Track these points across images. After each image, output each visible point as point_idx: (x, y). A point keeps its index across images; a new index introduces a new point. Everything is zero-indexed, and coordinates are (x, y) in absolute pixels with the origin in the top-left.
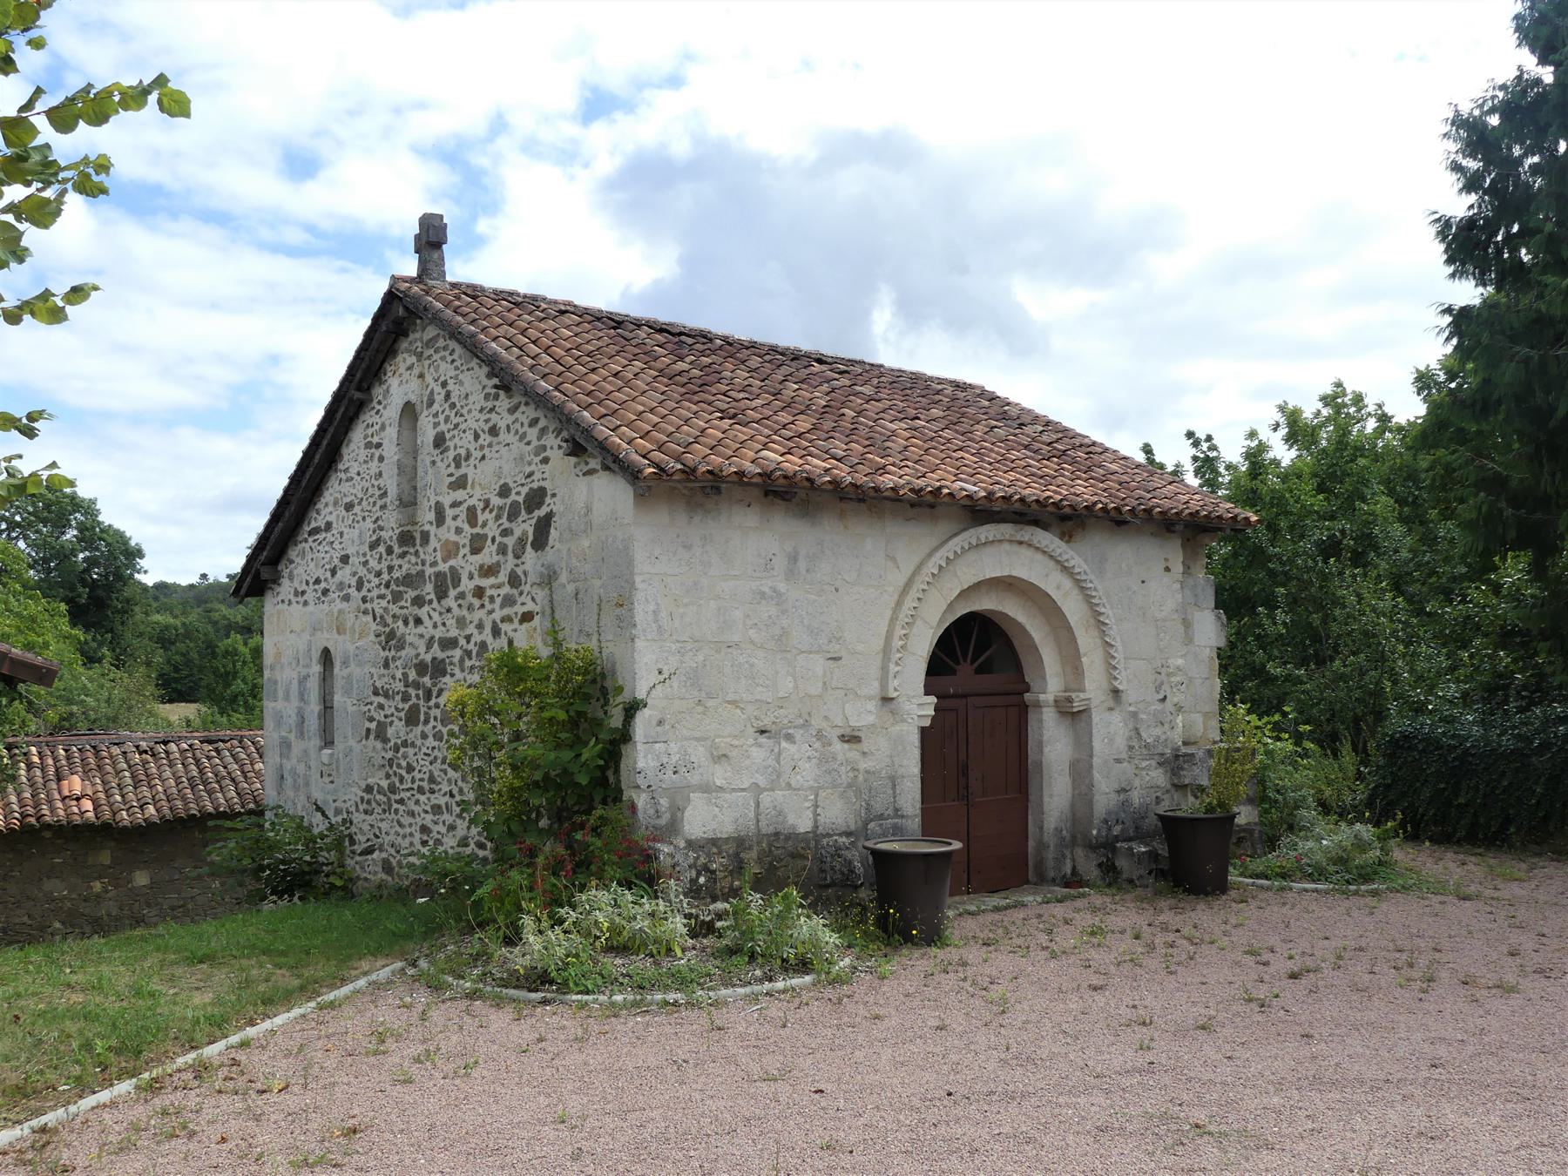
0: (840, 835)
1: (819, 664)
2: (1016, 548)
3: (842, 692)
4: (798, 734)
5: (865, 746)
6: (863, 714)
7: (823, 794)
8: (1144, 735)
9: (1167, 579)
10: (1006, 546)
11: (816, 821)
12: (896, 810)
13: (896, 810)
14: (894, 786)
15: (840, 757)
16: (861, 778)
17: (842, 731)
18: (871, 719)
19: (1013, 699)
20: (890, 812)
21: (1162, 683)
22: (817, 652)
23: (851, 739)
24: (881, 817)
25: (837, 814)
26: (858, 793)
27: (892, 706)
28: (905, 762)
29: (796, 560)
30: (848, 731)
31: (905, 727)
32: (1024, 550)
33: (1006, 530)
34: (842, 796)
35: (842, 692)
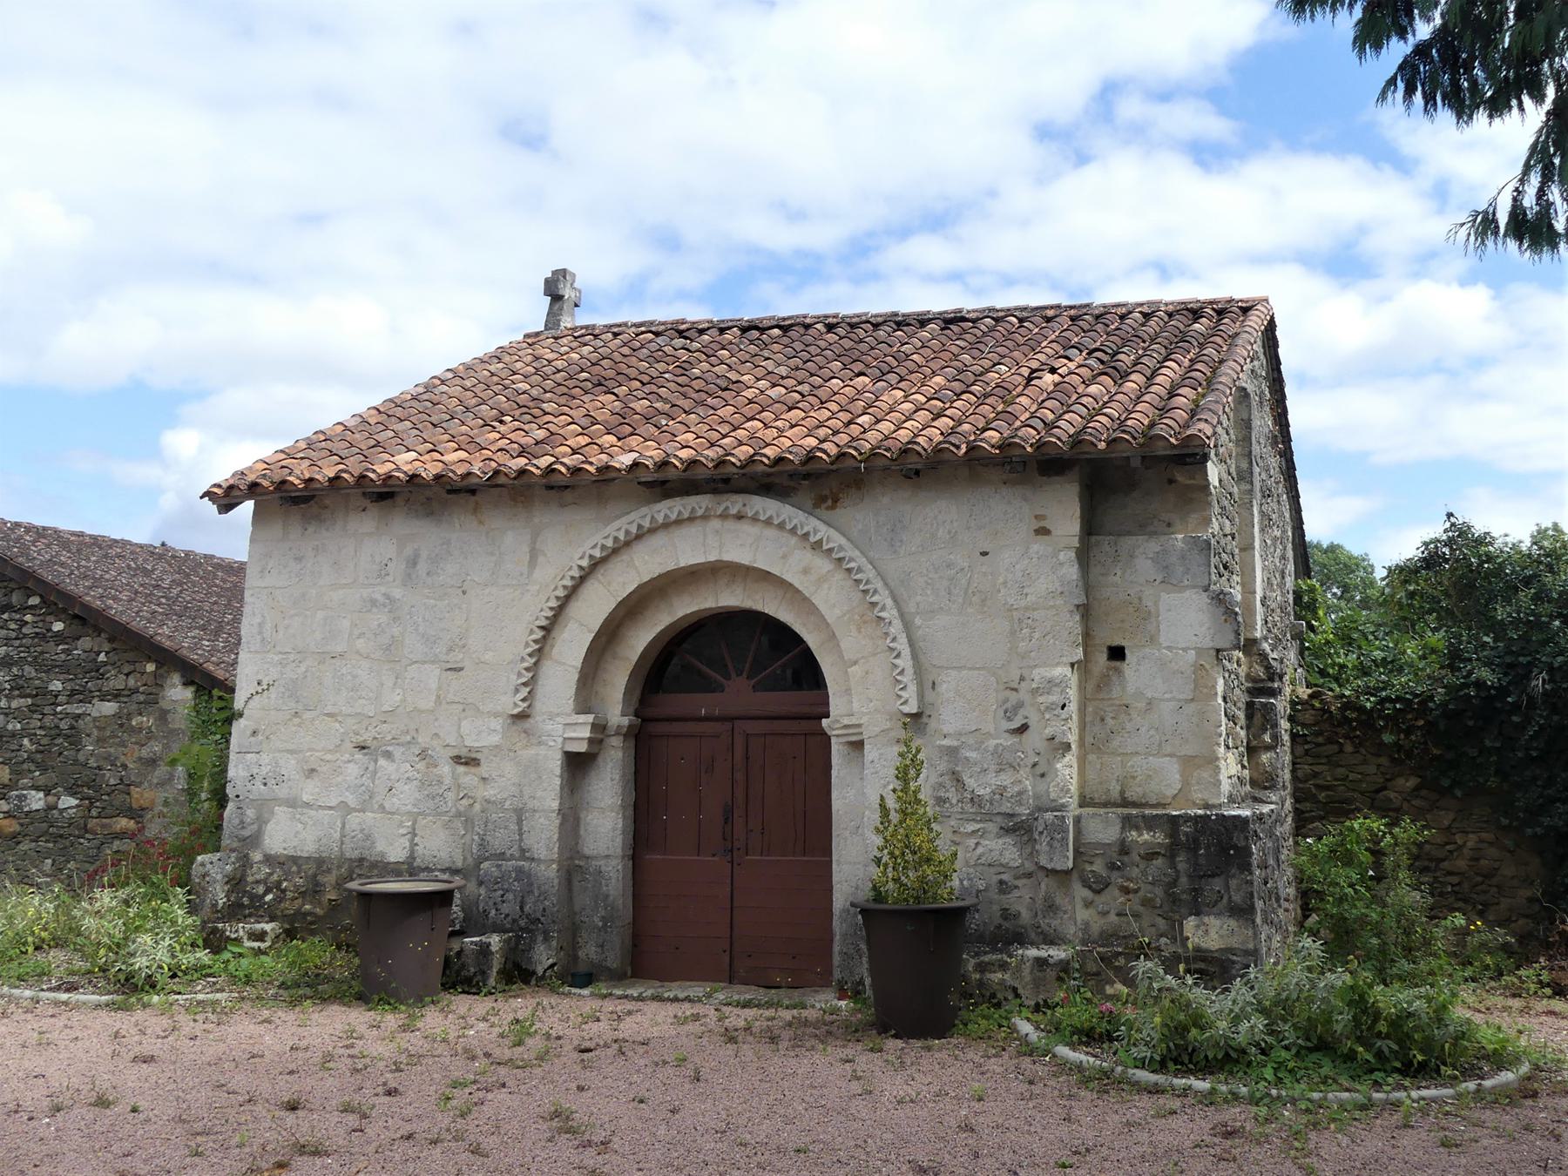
0: (443, 871)
1: (432, 675)
2: (731, 525)
3: (461, 707)
4: (398, 752)
5: (483, 770)
6: (484, 733)
7: (422, 822)
8: (971, 783)
9: (1039, 546)
10: (715, 524)
11: (412, 851)
12: (523, 851)
13: (523, 851)
14: (520, 822)
15: (447, 781)
16: (477, 807)
17: (455, 752)
18: (495, 739)
19: (805, 726)
20: (515, 851)
21: (1020, 705)
22: (433, 662)
23: (467, 760)
24: (502, 856)
25: (440, 845)
26: (469, 822)
27: (527, 724)
28: (539, 794)
29: (415, 564)
30: (464, 752)
31: (542, 751)
32: (746, 528)
33: (700, 503)
34: (446, 826)
35: (461, 707)
